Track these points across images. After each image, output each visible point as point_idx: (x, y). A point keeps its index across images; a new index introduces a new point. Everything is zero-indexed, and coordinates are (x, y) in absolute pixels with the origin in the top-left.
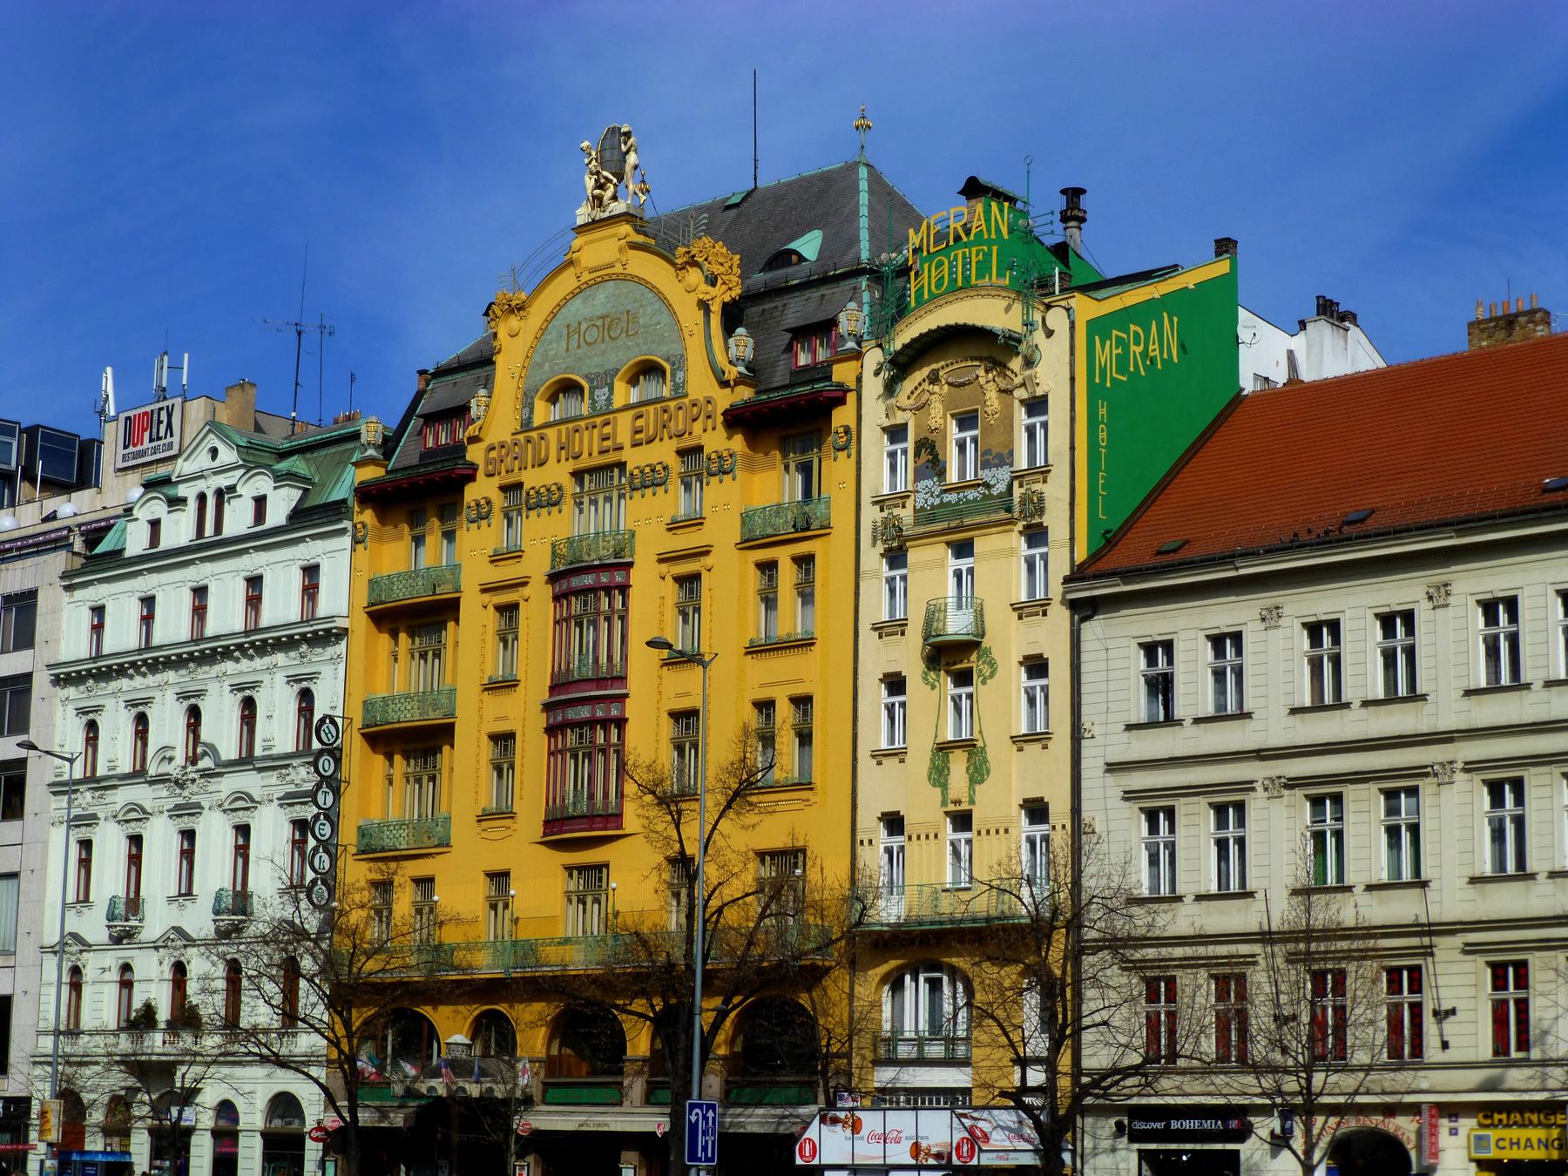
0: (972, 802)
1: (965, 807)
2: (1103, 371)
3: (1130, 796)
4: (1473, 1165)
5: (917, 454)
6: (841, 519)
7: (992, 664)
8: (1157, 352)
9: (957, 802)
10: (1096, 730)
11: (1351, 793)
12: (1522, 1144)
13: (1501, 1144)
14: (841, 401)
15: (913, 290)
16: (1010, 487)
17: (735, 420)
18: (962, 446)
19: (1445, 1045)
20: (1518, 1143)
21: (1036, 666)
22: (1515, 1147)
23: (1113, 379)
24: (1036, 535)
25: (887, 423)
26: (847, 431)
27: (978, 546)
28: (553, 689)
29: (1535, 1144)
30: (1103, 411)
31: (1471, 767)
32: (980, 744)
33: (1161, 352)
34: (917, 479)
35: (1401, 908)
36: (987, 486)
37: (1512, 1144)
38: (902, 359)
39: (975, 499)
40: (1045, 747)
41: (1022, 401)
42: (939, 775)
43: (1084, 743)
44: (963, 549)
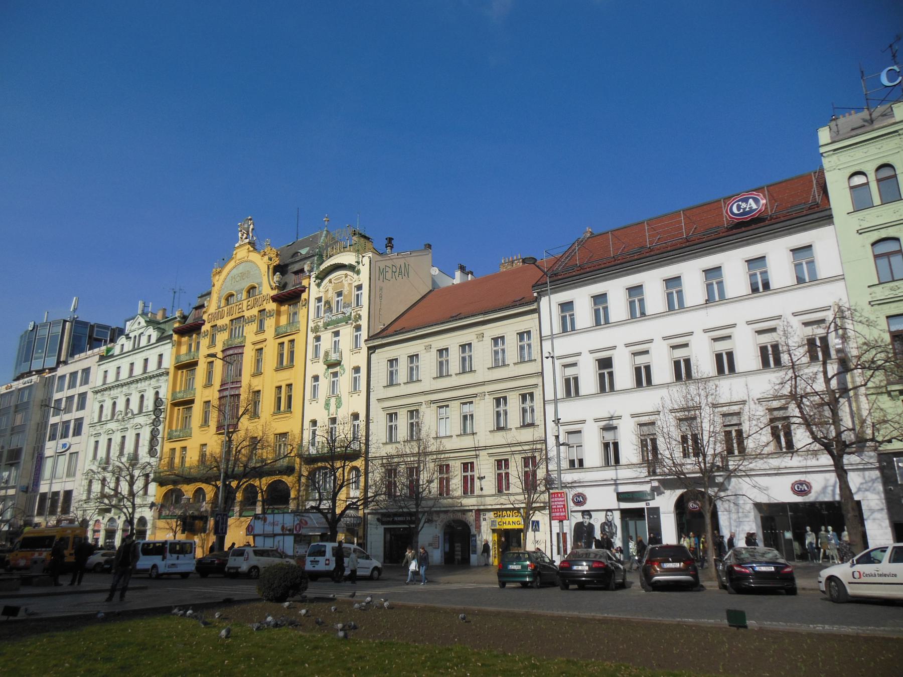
0: (336, 414)
1: (334, 416)
5: (325, 306)
6: (303, 327)
7: (344, 370)
10: (375, 389)
11: (451, 404)
12: (507, 523)
14: (304, 291)
16: (351, 313)
17: (275, 299)
19: (482, 489)
26: (305, 300)
28: (221, 386)
29: (511, 523)
31: (490, 393)
32: (340, 396)
34: (324, 313)
35: (467, 442)
36: (345, 314)
37: (503, 523)
38: (320, 276)
40: (359, 395)
42: (327, 405)
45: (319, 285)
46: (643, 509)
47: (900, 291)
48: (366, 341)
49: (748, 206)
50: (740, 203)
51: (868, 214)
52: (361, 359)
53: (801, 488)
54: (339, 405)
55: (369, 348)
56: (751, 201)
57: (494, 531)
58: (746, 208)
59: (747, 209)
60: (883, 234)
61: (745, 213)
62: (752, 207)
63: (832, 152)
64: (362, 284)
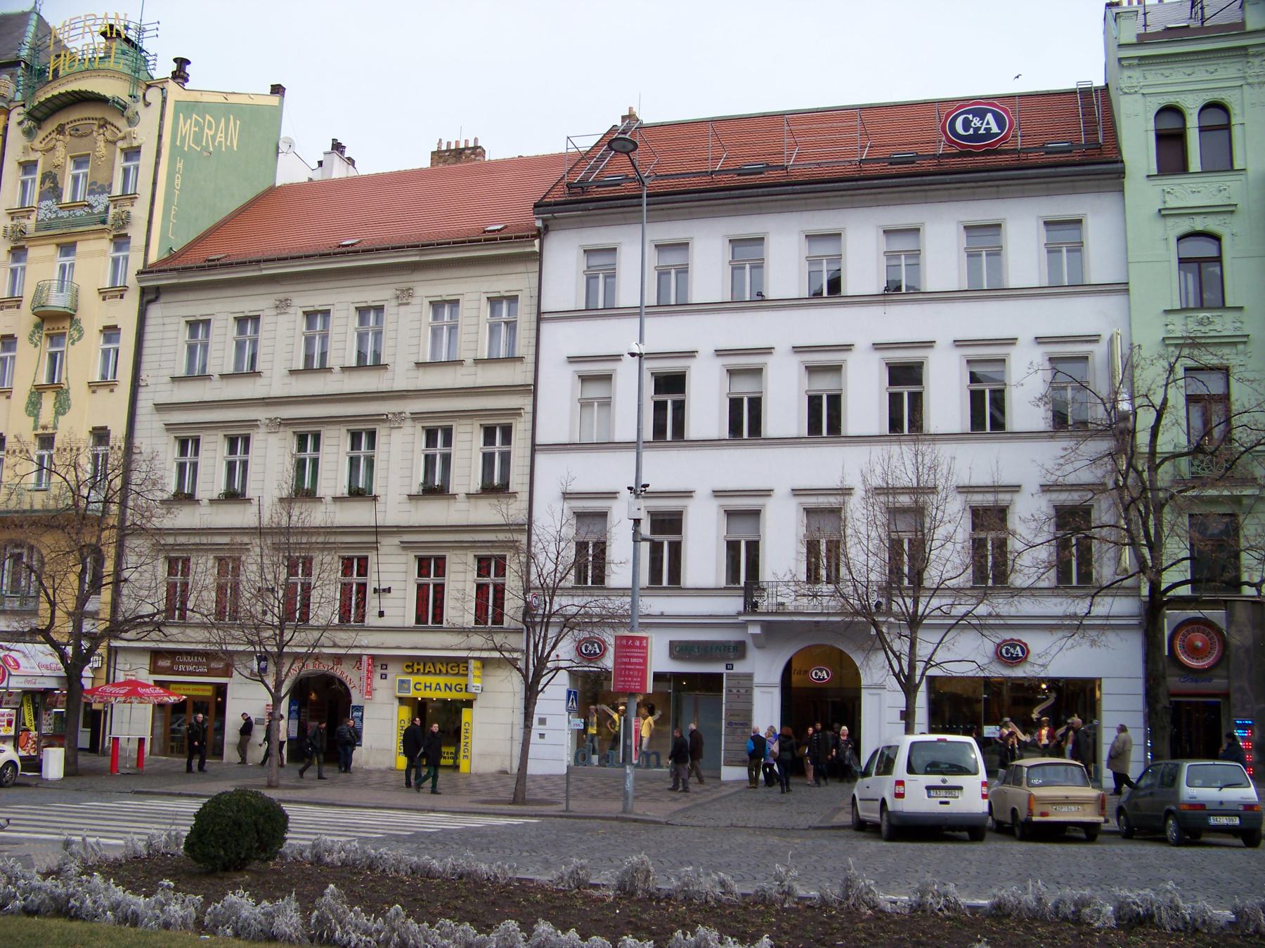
0: (55, 428)
1: (50, 431)
2: (183, 139)
3: (170, 427)
4: (396, 702)
5: (43, 182)
7: (80, 331)
8: (223, 139)
9: (45, 428)
10: (150, 381)
13: (418, 686)
15: (52, 69)
16: (107, 208)
18: (76, 179)
19: (381, 614)
20: (430, 687)
21: (111, 332)
22: (428, 689)
23: (189, 145)
24: (121, 241)
25: (22, 160)
27: (81, 247)
29: (442, 686)
30: (180, 165)
31: (416, 417)
32: (65, 387)
33: (226, 139)
34: (40, 200)
35: (358, 514)
36: (90, 206)
37: (426, 687)
39: (81, 215)
40: (112, 391)
41: (122, 150)
42: (34, 406)
43: (141, 390)
44: (67, 249)
45: (29, 133)
46: (721, 675)
47: (1211, 327)
48: (139, 273)
49: (984, 126)
50: (970, 117)
51: (1180, 185)
52: (125, 313)
53: (1011, 654)
54: (62, 407)
55: (144, 291)
56: (989, 117)
57: (402, 701)
58: (979, 128)
59: (982, 131)
60: (1199, 224)
61: (976, 137)
62: (990, 129)
63: (1136, 62)
64: (139, 147)
